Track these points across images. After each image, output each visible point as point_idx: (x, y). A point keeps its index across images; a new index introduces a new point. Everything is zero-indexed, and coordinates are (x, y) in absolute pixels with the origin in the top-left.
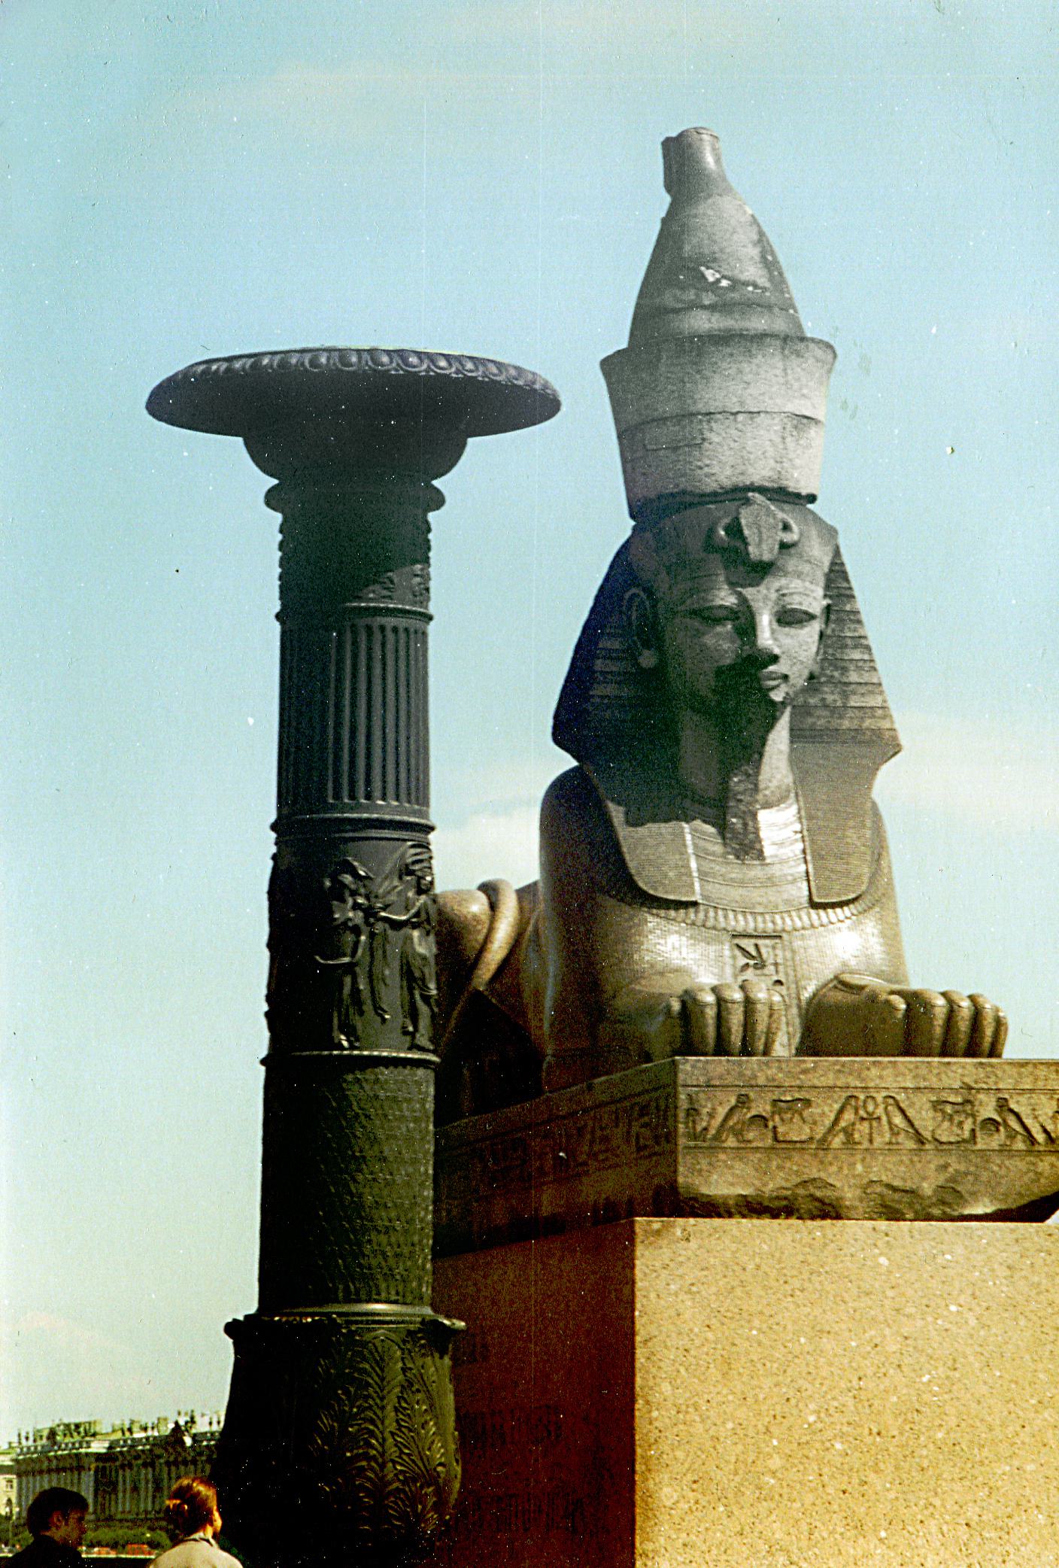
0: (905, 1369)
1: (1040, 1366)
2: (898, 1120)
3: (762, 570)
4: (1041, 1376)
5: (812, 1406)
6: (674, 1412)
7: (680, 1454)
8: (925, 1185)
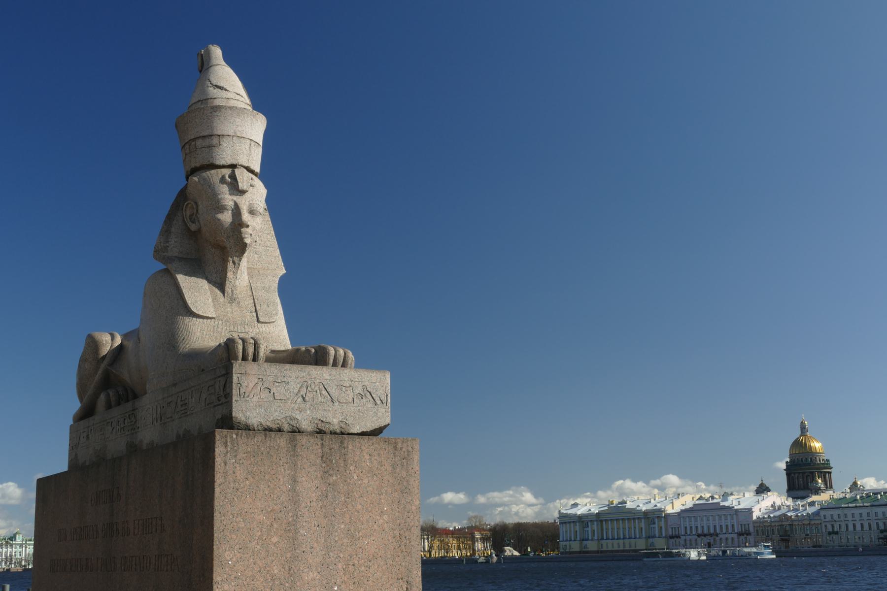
1: (382, 497)
2: (324, 392)
3: (243, 192)
5: (291, 514)
7: (234, 536)
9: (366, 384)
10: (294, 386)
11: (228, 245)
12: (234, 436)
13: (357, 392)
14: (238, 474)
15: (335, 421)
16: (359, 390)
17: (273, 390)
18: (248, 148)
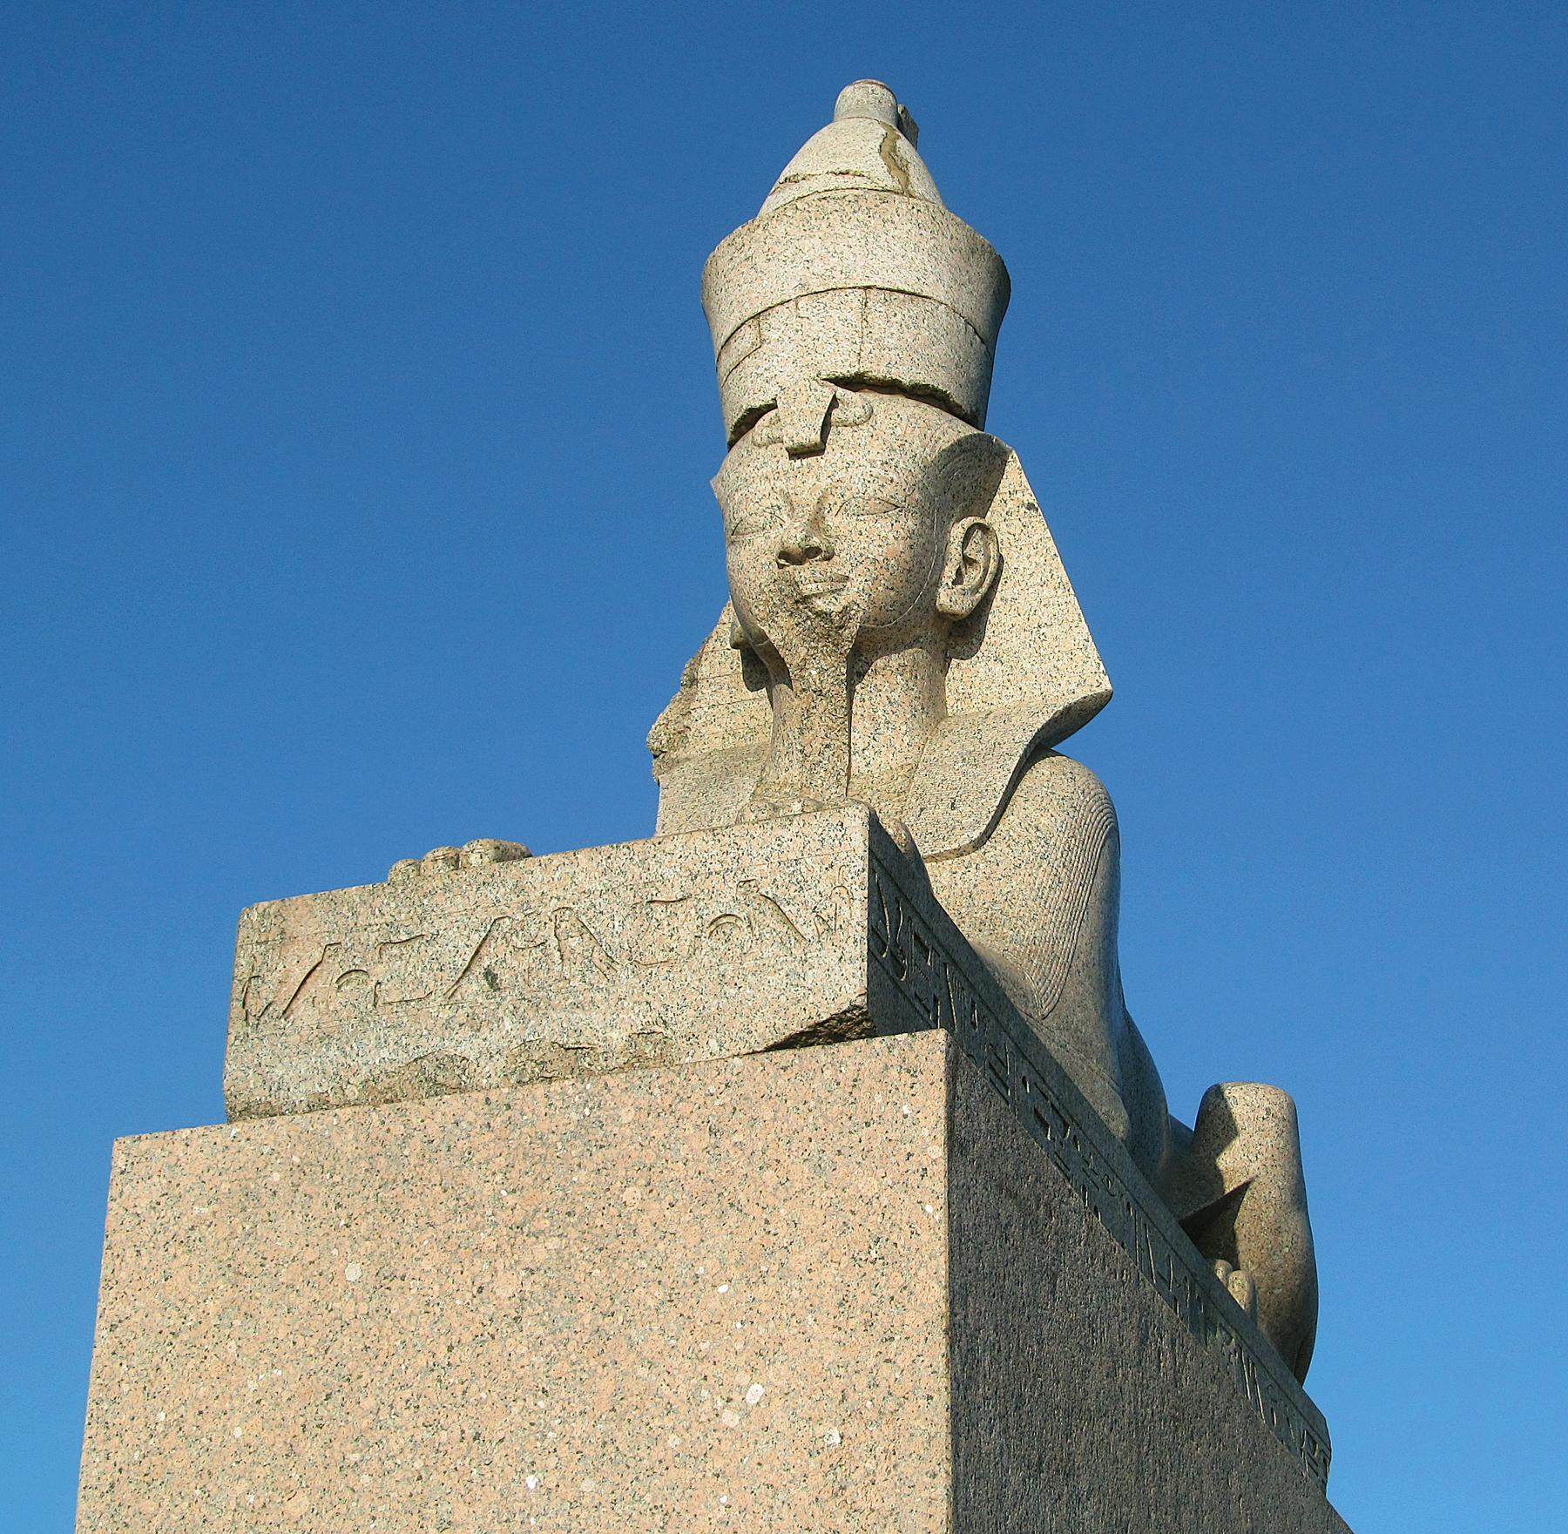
0: (527, 1323)
4: (763, 1308)
5: (370, 1403)
6: (144, 1437)
8: (614, 1035)
9: (754, 873)
10: (457, 945)
11: (774, 637)
12: (179, 1149)
13: (715, 910)
14: (180, 1279)
15: (617, 1037)
16: (726, 897)
17: (380, 971)
18: (854, 317)
